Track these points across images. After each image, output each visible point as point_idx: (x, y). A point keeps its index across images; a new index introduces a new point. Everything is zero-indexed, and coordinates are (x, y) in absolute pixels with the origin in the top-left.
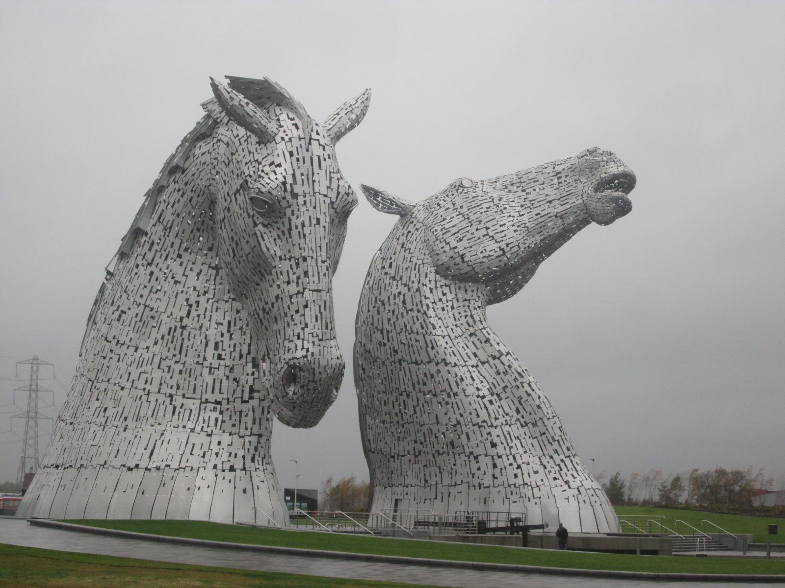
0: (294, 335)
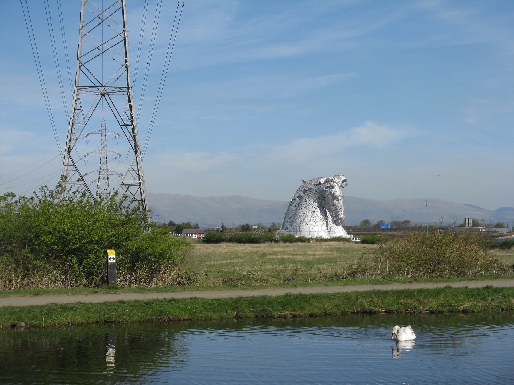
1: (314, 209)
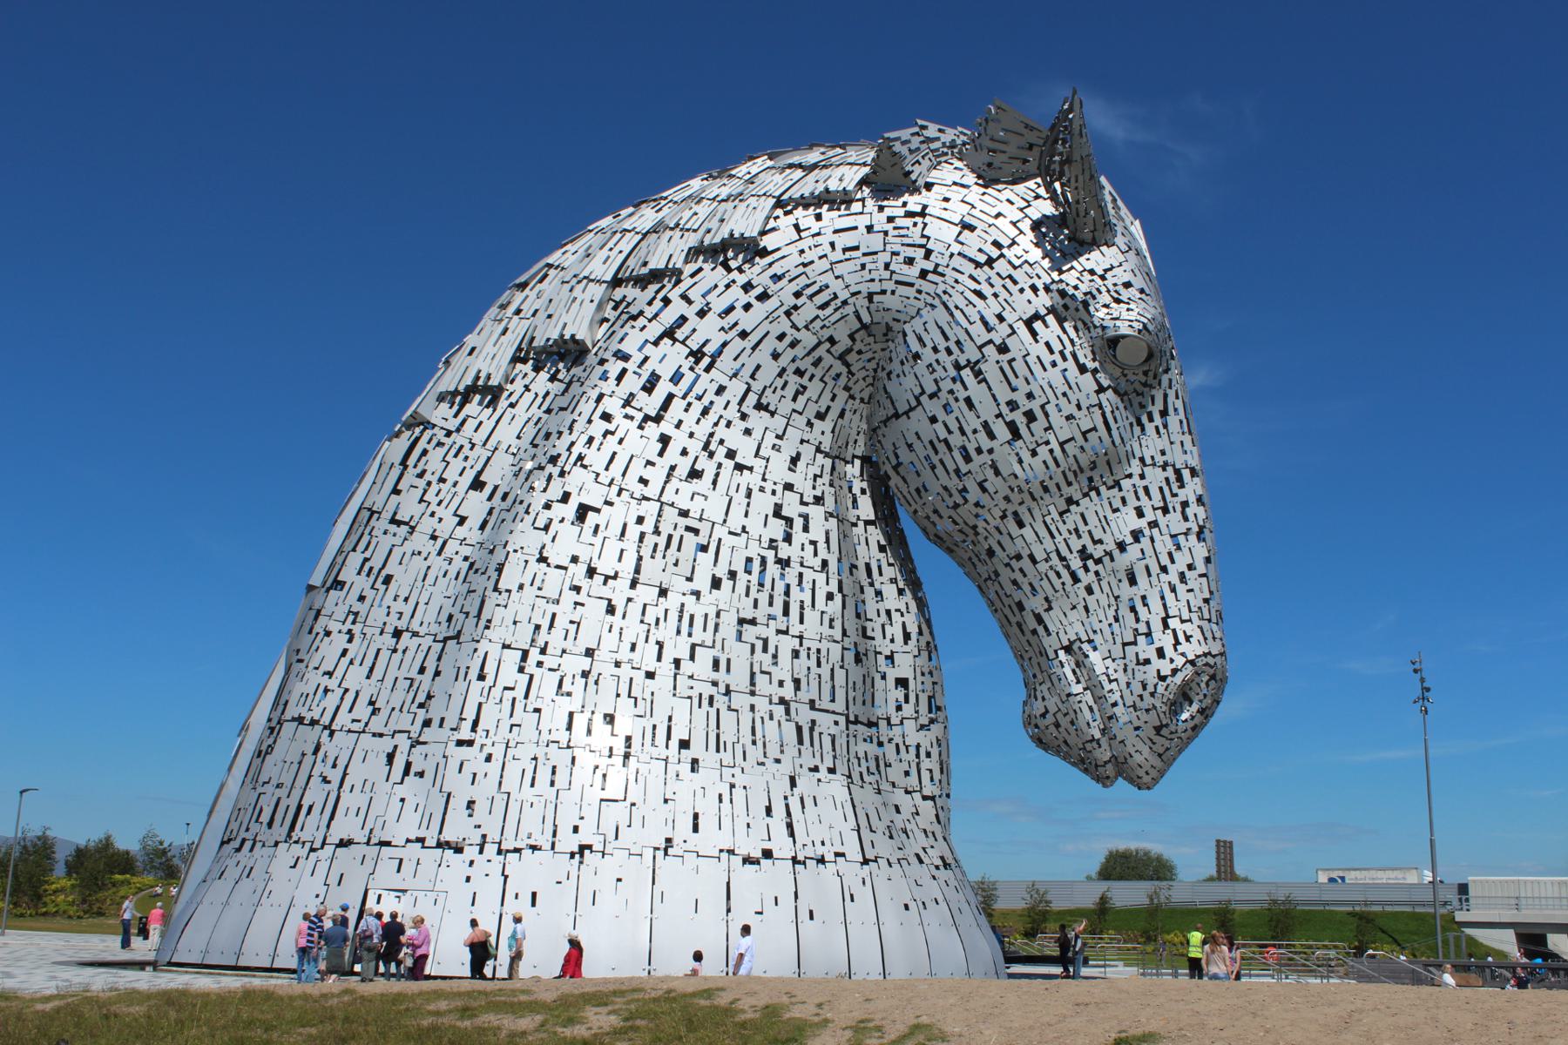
0: (1190, 611)
1: (777, 528)
